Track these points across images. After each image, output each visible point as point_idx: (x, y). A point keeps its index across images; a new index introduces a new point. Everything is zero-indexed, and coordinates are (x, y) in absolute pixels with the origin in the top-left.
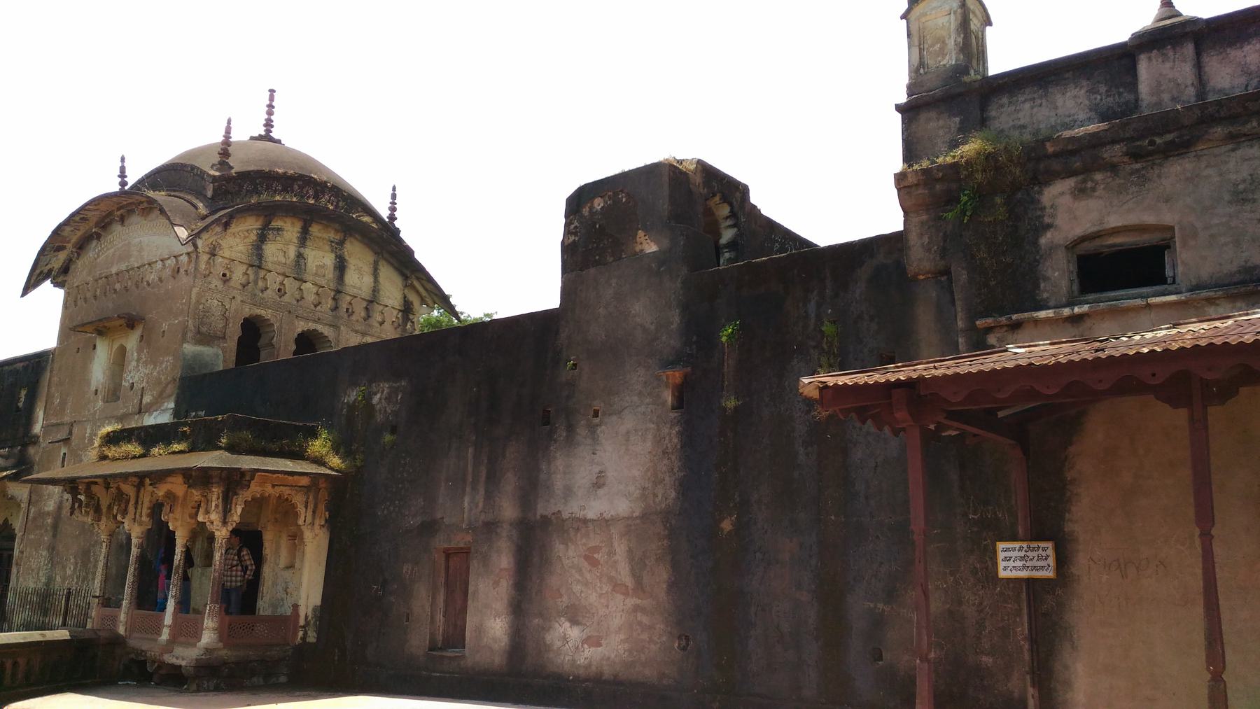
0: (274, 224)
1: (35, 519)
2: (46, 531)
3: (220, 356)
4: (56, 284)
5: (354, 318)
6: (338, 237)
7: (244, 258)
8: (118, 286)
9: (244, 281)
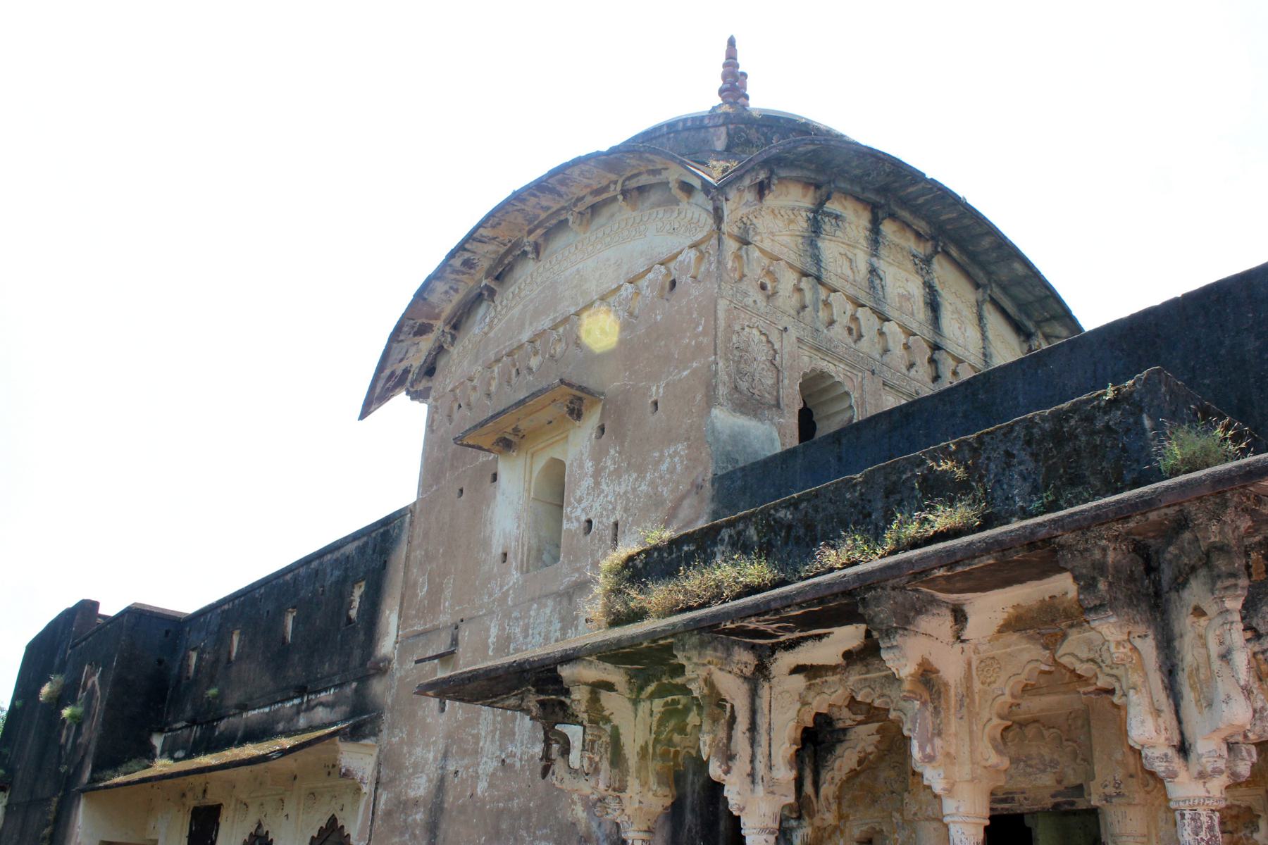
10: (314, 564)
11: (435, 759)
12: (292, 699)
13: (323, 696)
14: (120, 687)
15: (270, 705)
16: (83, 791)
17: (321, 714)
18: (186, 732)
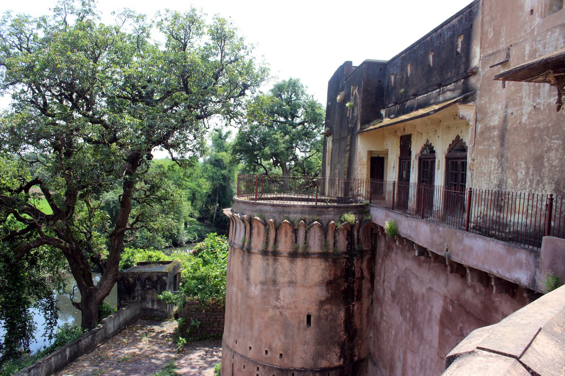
1: (482, 133)
2: (494, 141)
10: (439, 31)
11: (502, 109)
12: (436, 89)
14: (366, 92)
15: (427, 93)
16: (359, 133)
17: (449, 94)
18: (394, 107)
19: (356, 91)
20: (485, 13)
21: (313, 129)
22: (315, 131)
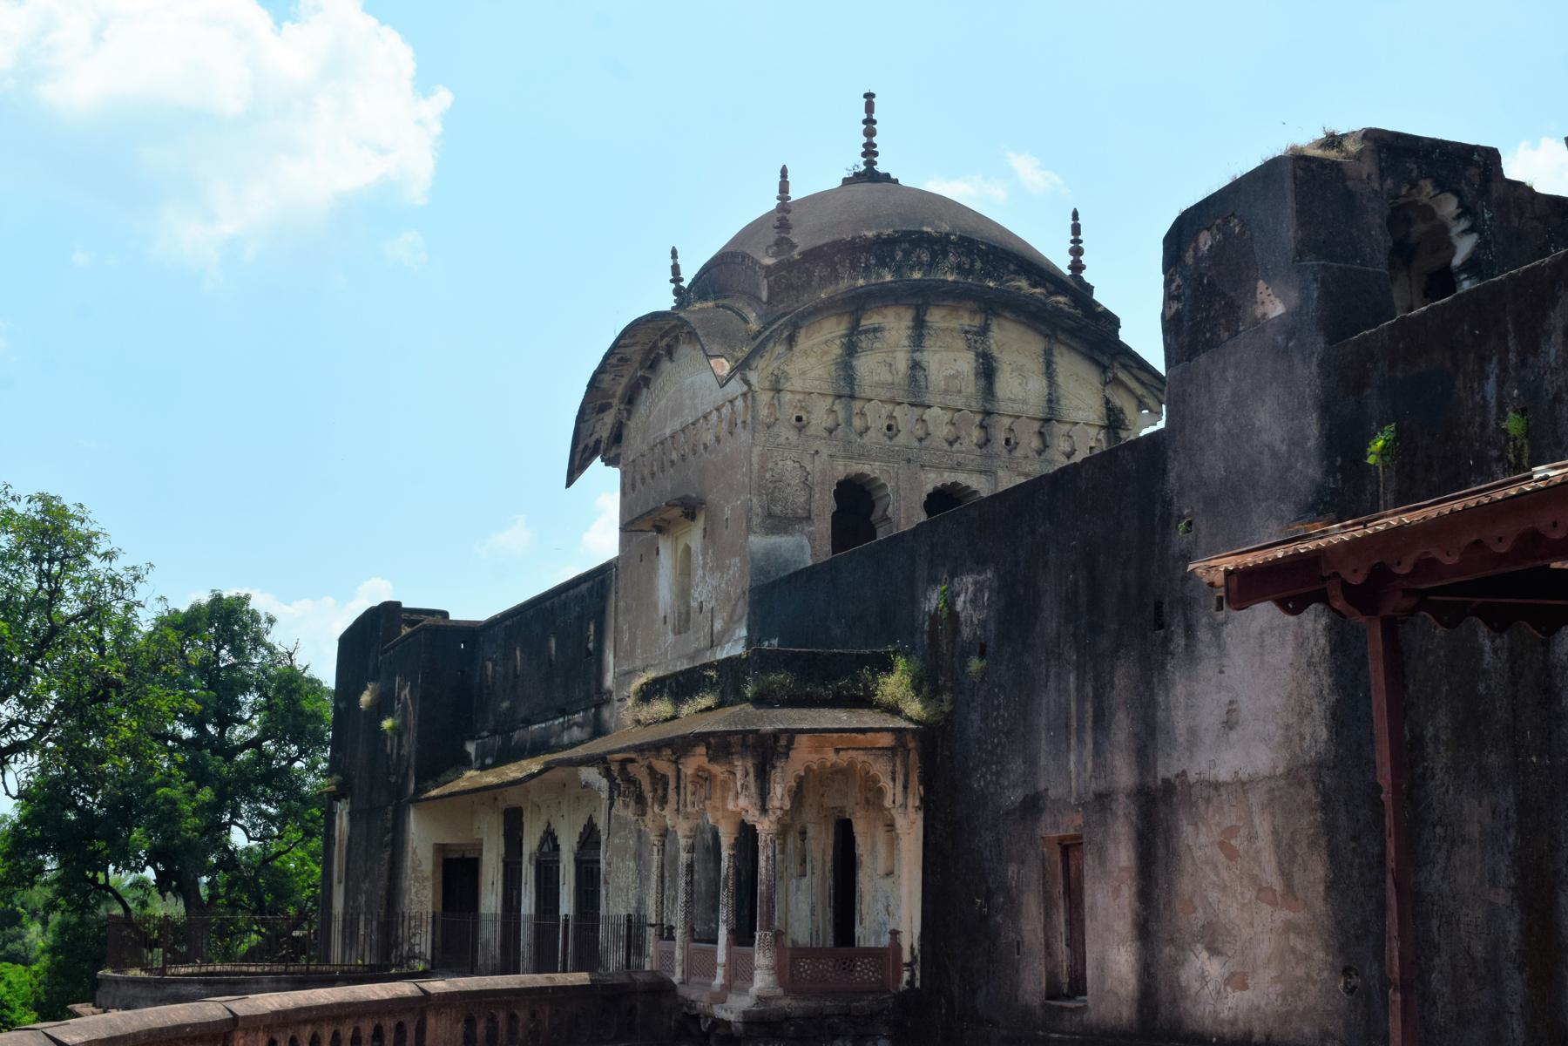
0: (866, 323)
3: (805, 547)
4: (609, 462)
5: (1019, 453)
6: (977, 322)
7: (825, 387)
8: (674, 456)
9: (830, 423)
13: (578, 717)
16: (410, 802)
18: (491, 740)
19: (407, 691)
20: (621, 593)
21: (292, 761)
22: (298, 765)
